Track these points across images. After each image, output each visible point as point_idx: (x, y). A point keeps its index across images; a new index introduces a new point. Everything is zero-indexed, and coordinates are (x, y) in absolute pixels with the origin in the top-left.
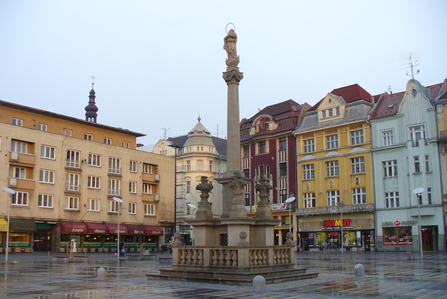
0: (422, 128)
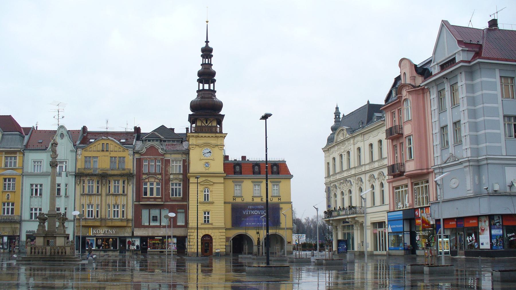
0: (64, 163)
